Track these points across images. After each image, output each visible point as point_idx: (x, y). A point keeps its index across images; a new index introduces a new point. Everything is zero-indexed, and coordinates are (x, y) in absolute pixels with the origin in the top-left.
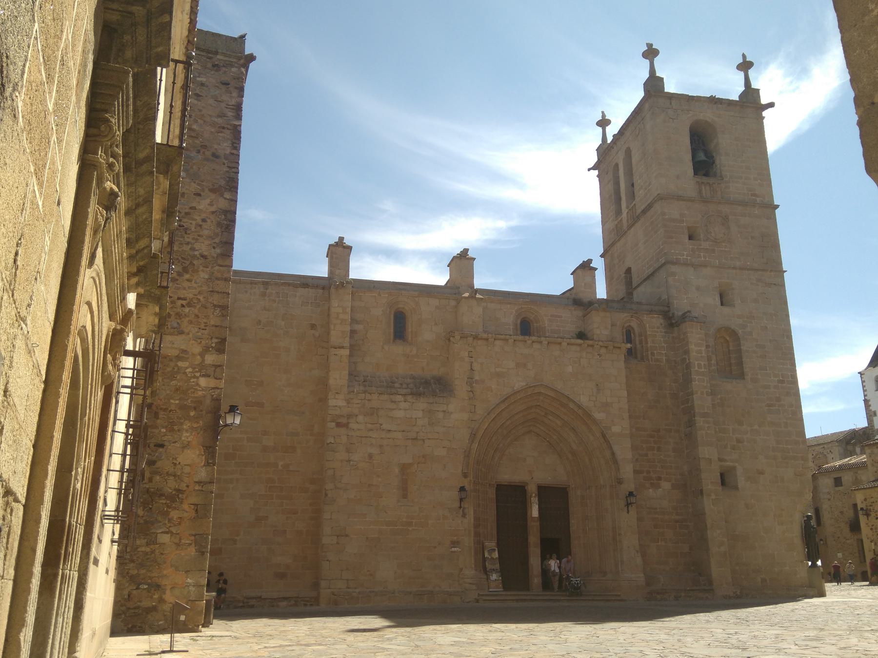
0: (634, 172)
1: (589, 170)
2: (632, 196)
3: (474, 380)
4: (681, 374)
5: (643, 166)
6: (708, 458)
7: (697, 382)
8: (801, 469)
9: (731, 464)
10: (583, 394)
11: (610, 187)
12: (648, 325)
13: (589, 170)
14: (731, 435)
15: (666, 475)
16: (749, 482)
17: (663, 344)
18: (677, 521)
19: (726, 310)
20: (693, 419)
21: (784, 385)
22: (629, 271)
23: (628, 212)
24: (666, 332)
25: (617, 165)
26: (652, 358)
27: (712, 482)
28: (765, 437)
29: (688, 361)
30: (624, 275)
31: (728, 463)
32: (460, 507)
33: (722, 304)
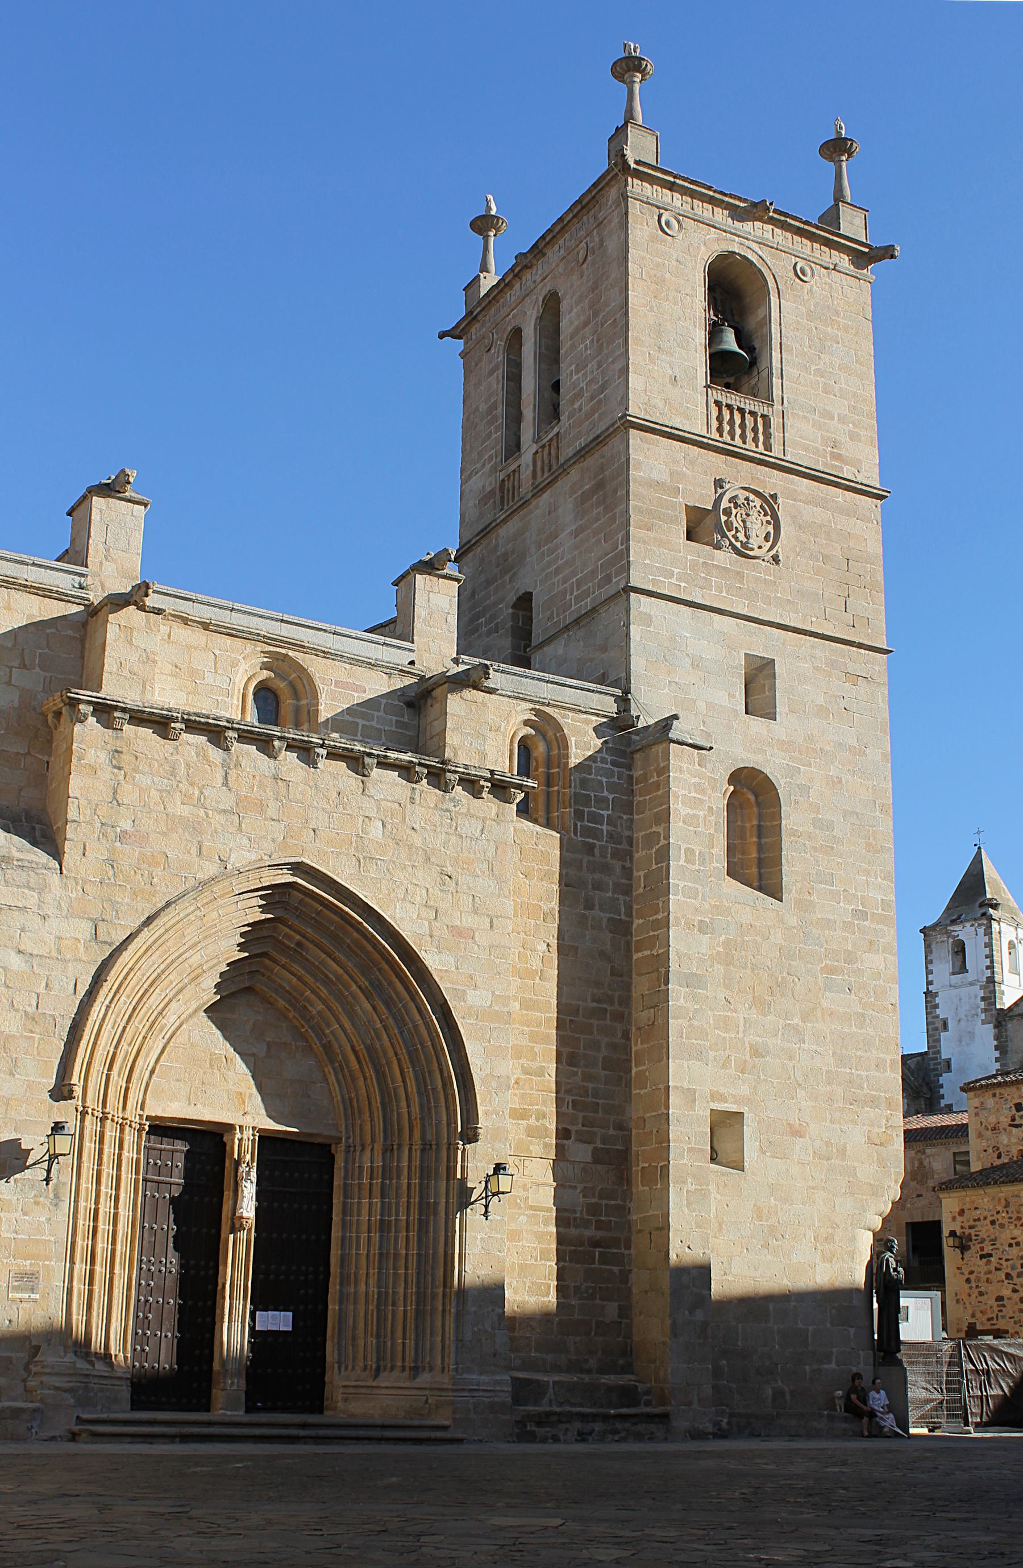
0: (562, 352)
1: (442, 336)
2: (551, 412)
4: (642, 873)
5: (588, 342)
9: (733, 1108)
11: (496, 385)
12: (573, 739)
13: (442, 336)
15: (583, 1126)
17: (606, 793)
18: (596, 1244)
19: (757, 724)
20: (663, 987)
22: (525, 601)
23: (537, 452)
24: (614, 763)
25: (517, 334)
26: (575, 825)
27: (690, 1150)
29: (663, 842)
30: (510, 611)
32: (47, 1180)
33: (747, 713)
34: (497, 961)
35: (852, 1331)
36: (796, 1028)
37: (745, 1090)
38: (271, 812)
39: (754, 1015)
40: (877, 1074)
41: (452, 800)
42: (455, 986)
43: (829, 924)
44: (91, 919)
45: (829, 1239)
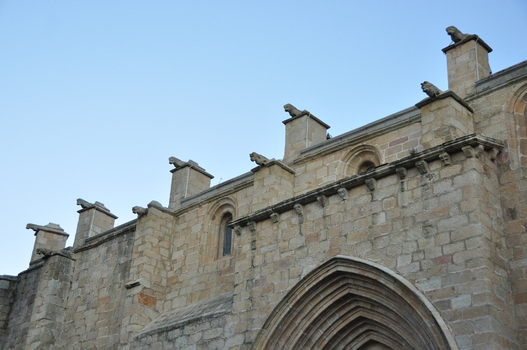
3: (254, 280)
10: (402, 254)
34: (472, 270)
38: (322, 237)
41: (427, 177)
42: (442, 300)
44: (243, 333)
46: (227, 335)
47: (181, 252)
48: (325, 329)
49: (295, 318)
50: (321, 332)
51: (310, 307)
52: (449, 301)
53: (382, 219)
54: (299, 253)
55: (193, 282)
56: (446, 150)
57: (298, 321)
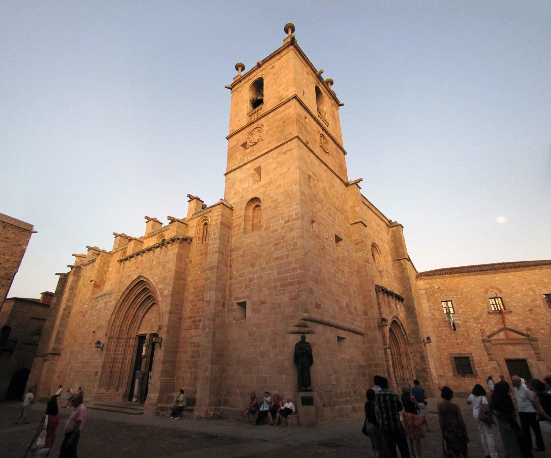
6: (209, 300)
7: (211, 246)
8: (296, 293)
14: (246, 277)
16: (253, 313)
21: (289, 223)
27: (208, 319)
28: (270, 272)
31: (241, 300)
35: (284, 376)
36: (263, 268)
37: (247, 294)
38: (140, 268)
39: (251, 269)
40: (293, 273)
43: (276, 230)
45: (275, 340)
46: (112, 300)
47: (111, 268)
48: (140, 299)
49: (131, 295)
50: (139, 300)
51: (135, 292)
52: (163, 292)
53: (154, 263)
54: (134, 273)
55: (113, 280)
56: (171, 240)
57: (131, 296)
